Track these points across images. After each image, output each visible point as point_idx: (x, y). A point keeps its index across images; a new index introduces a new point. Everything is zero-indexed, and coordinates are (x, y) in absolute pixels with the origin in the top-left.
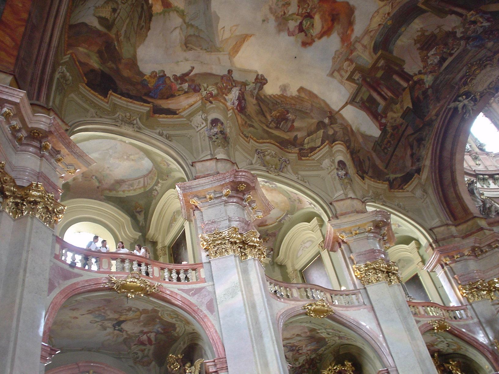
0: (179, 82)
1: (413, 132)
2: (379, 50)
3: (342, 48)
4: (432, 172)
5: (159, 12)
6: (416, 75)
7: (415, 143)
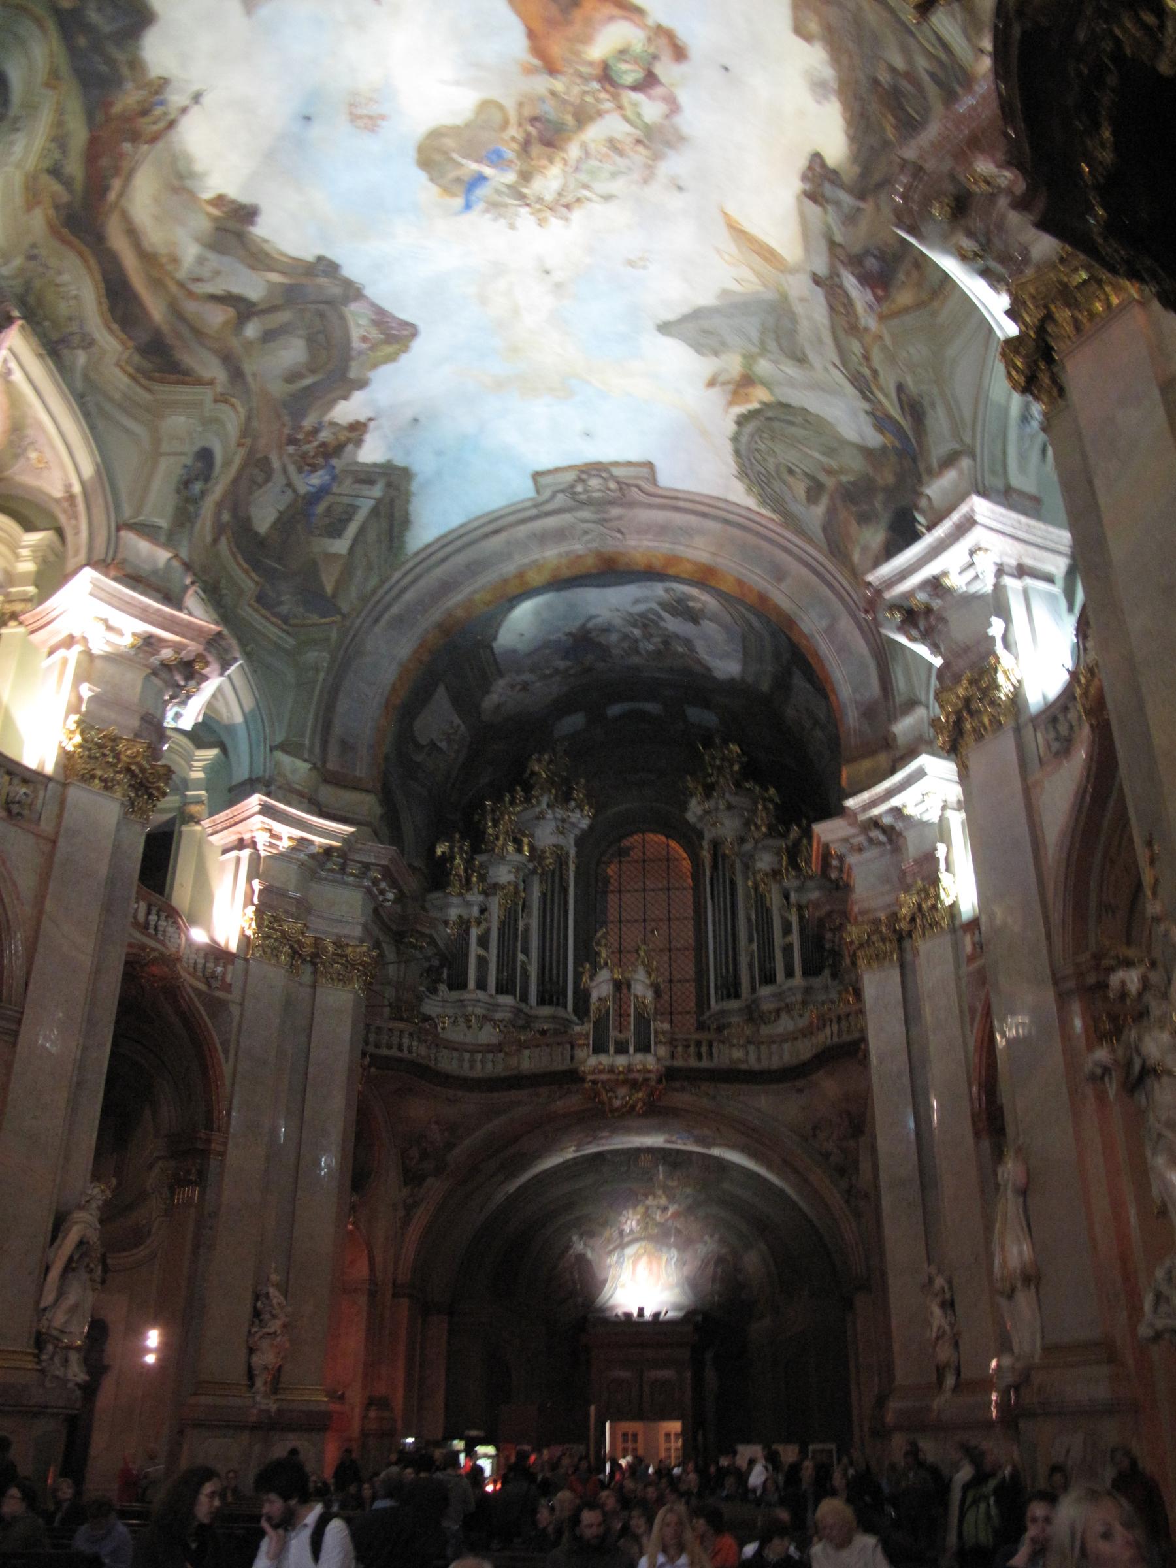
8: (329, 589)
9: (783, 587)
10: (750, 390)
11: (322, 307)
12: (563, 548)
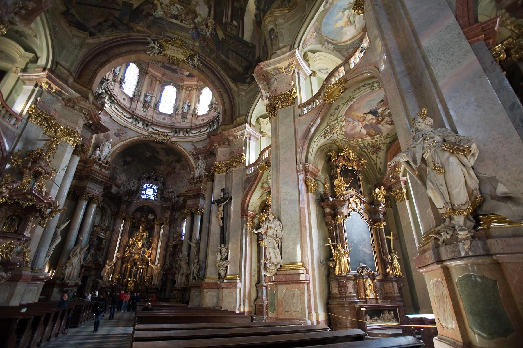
1: (117, 17)
4: (97, 46)
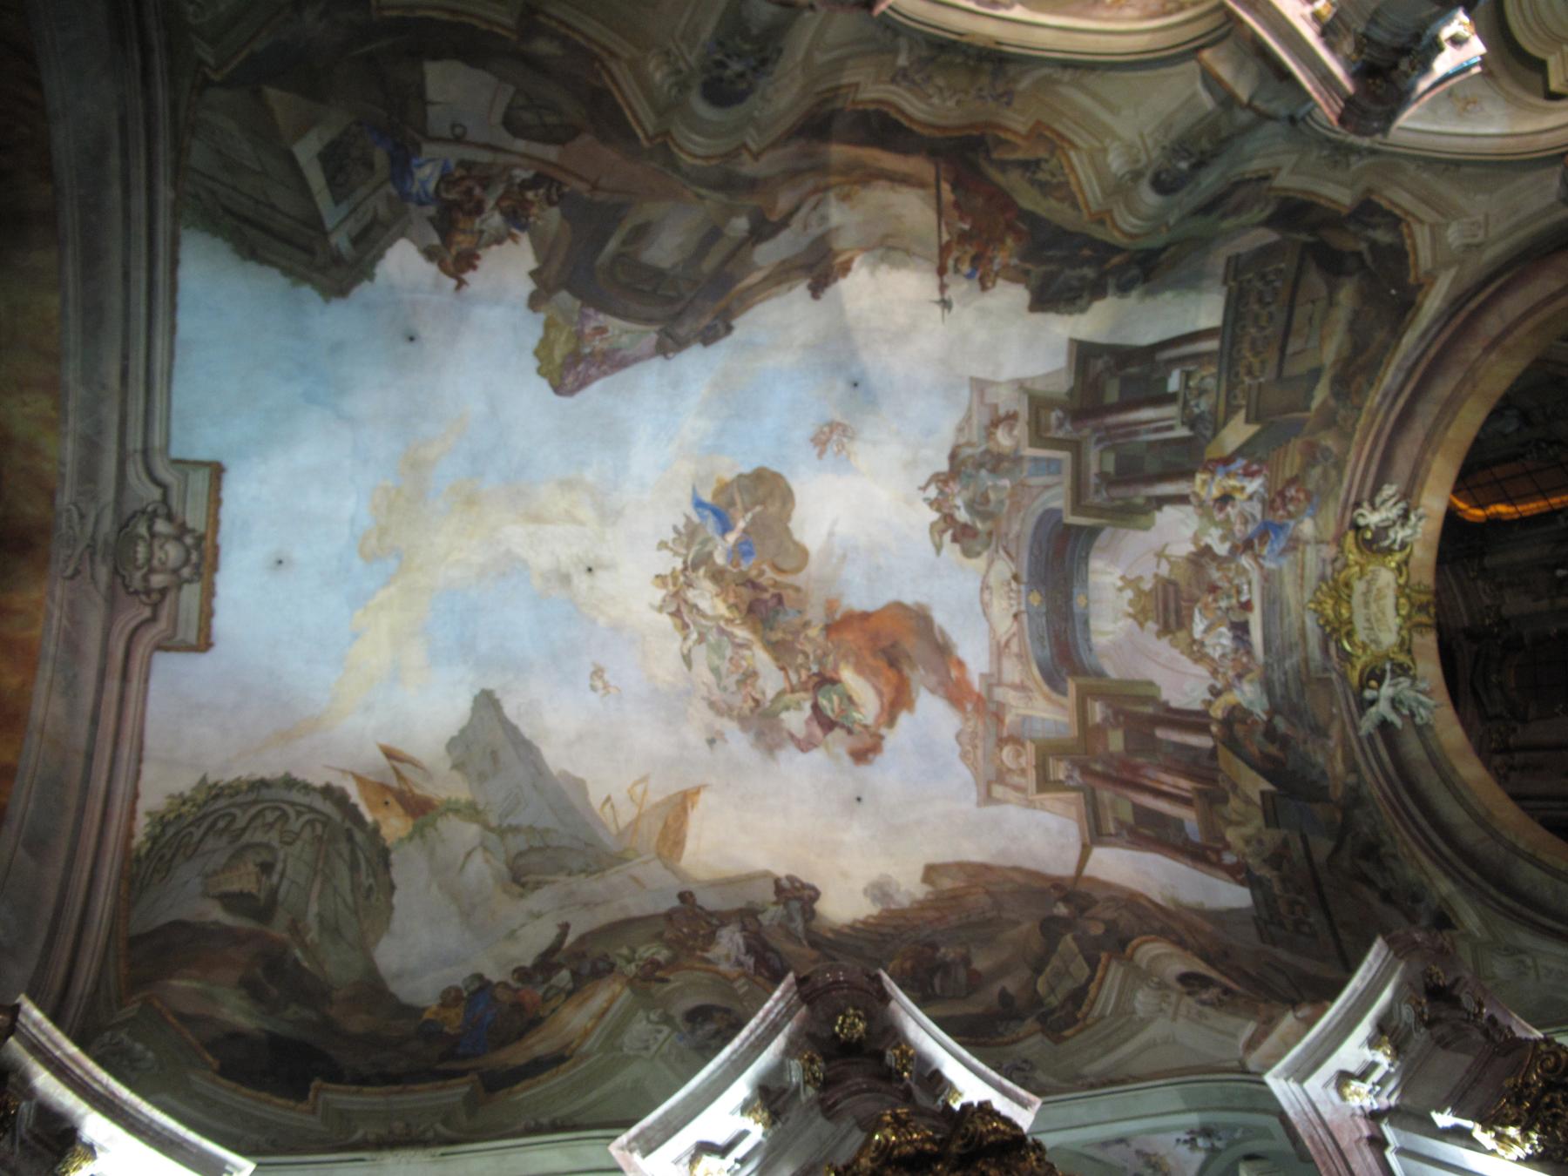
0: (539, 978)
2: (1065, 681)
3: (967, 720)
5: (403, 834)
6: (1209, 703)
7: (1365, 866)
8: (272, 93)
9: (21, 852)
10: (399, 809)
11: (678, 307)
12: (70, 470)
